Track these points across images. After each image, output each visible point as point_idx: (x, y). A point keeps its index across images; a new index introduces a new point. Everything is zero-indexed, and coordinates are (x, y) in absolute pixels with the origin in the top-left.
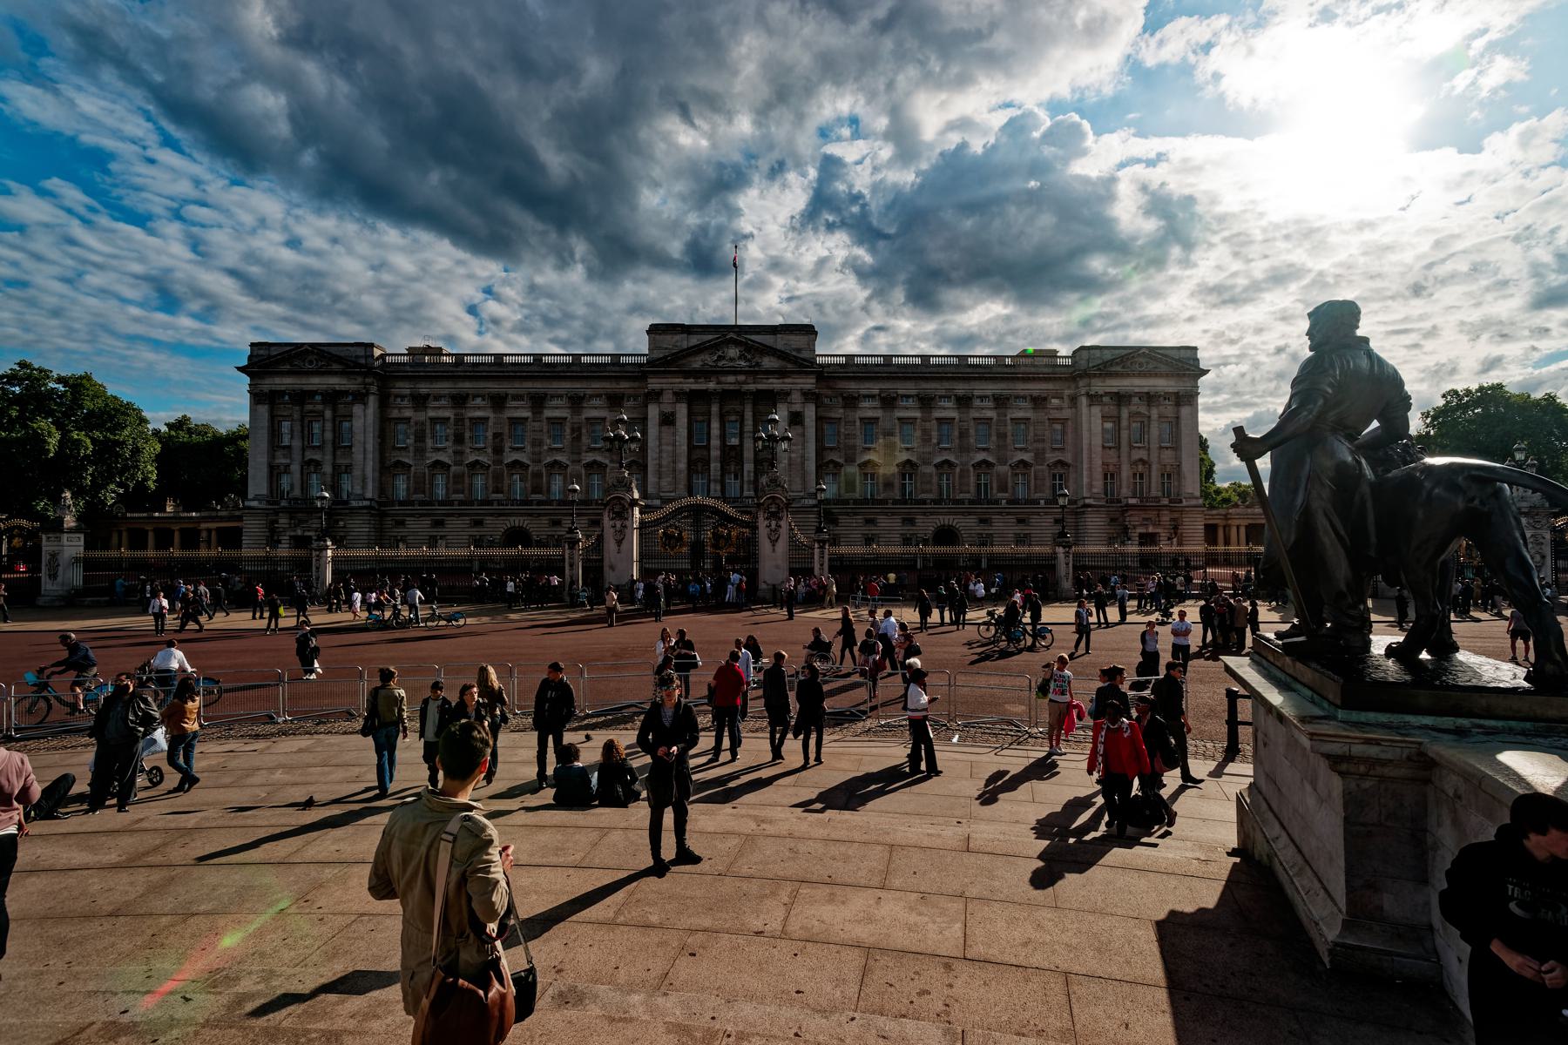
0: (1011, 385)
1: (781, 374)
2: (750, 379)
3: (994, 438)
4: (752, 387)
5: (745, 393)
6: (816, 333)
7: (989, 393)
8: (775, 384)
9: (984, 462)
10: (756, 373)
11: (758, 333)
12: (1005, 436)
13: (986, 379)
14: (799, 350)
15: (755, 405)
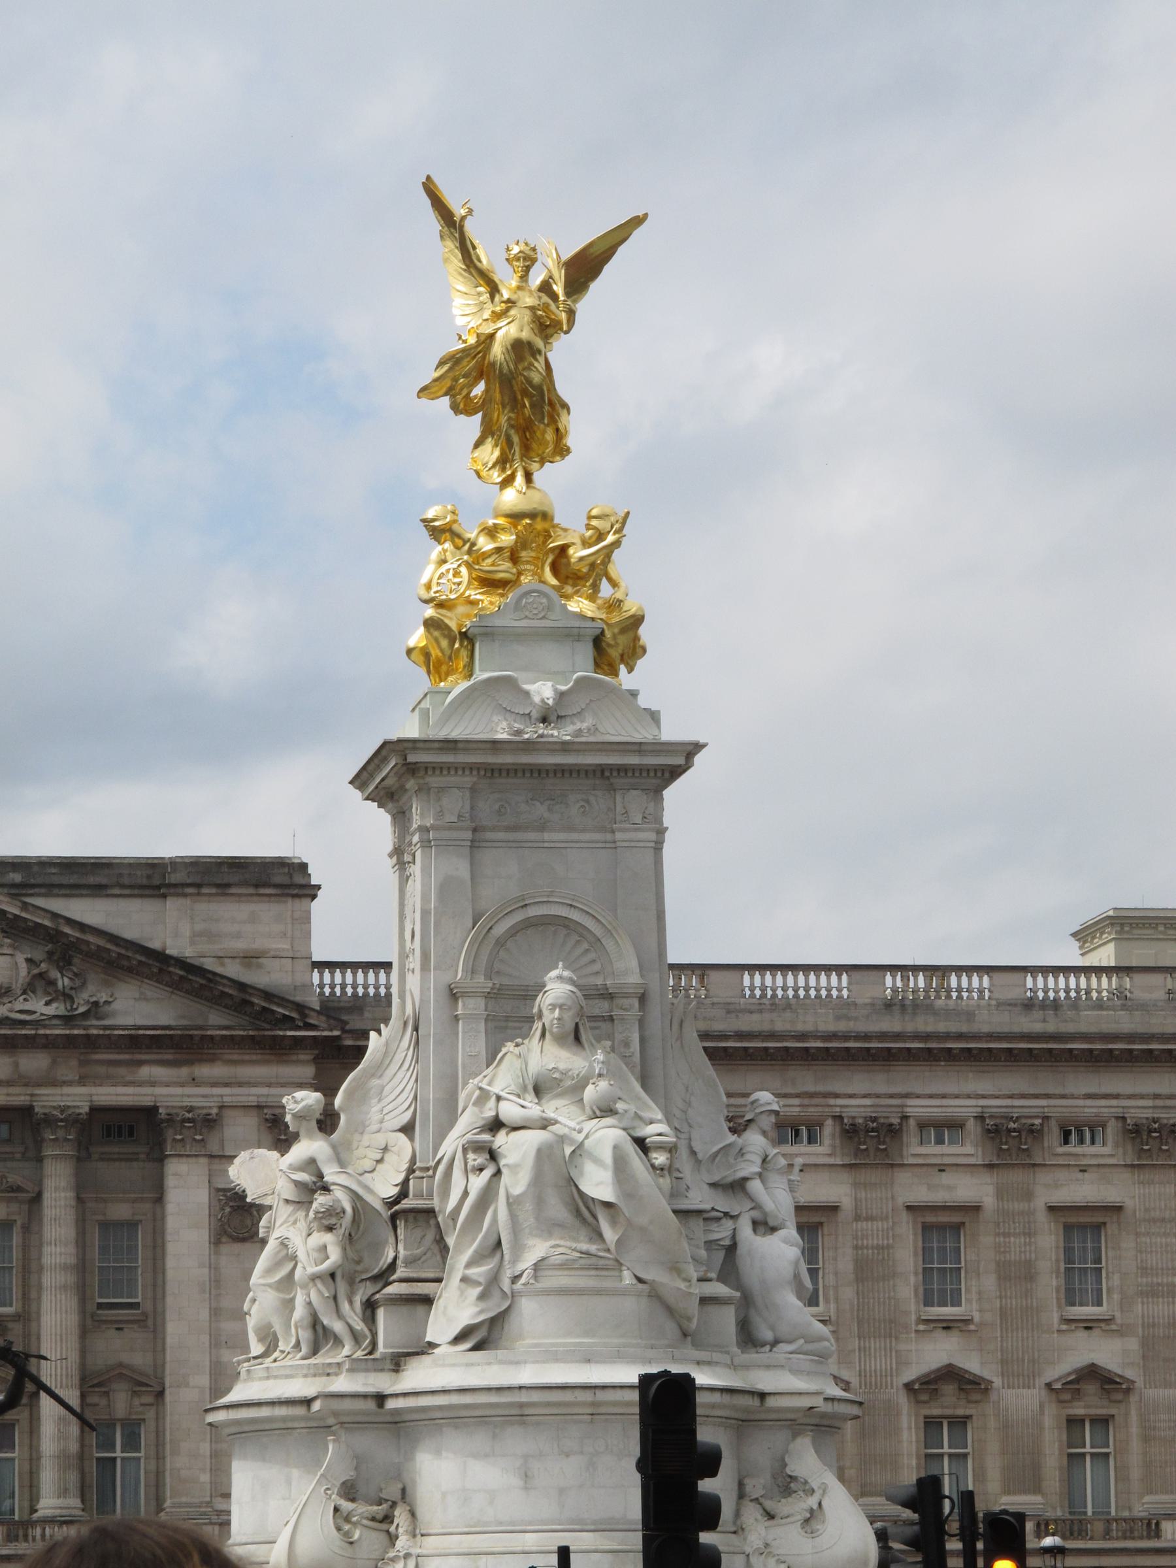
0: (1047, 1081)
1: (183, 1047)
2: (68, 1069)
3: (989, 1282)
4: (78, 1097)
5: (49, 1121)
6: (310, 892)
7: (964, 1108)
8: (160, 1087)
9: (950, 1374)
10: (91, 1043)
11: (98, 890)
12: (1026, 1273)
13: (949, 1056)
14: (250, 958)
15: (82, 1157)
